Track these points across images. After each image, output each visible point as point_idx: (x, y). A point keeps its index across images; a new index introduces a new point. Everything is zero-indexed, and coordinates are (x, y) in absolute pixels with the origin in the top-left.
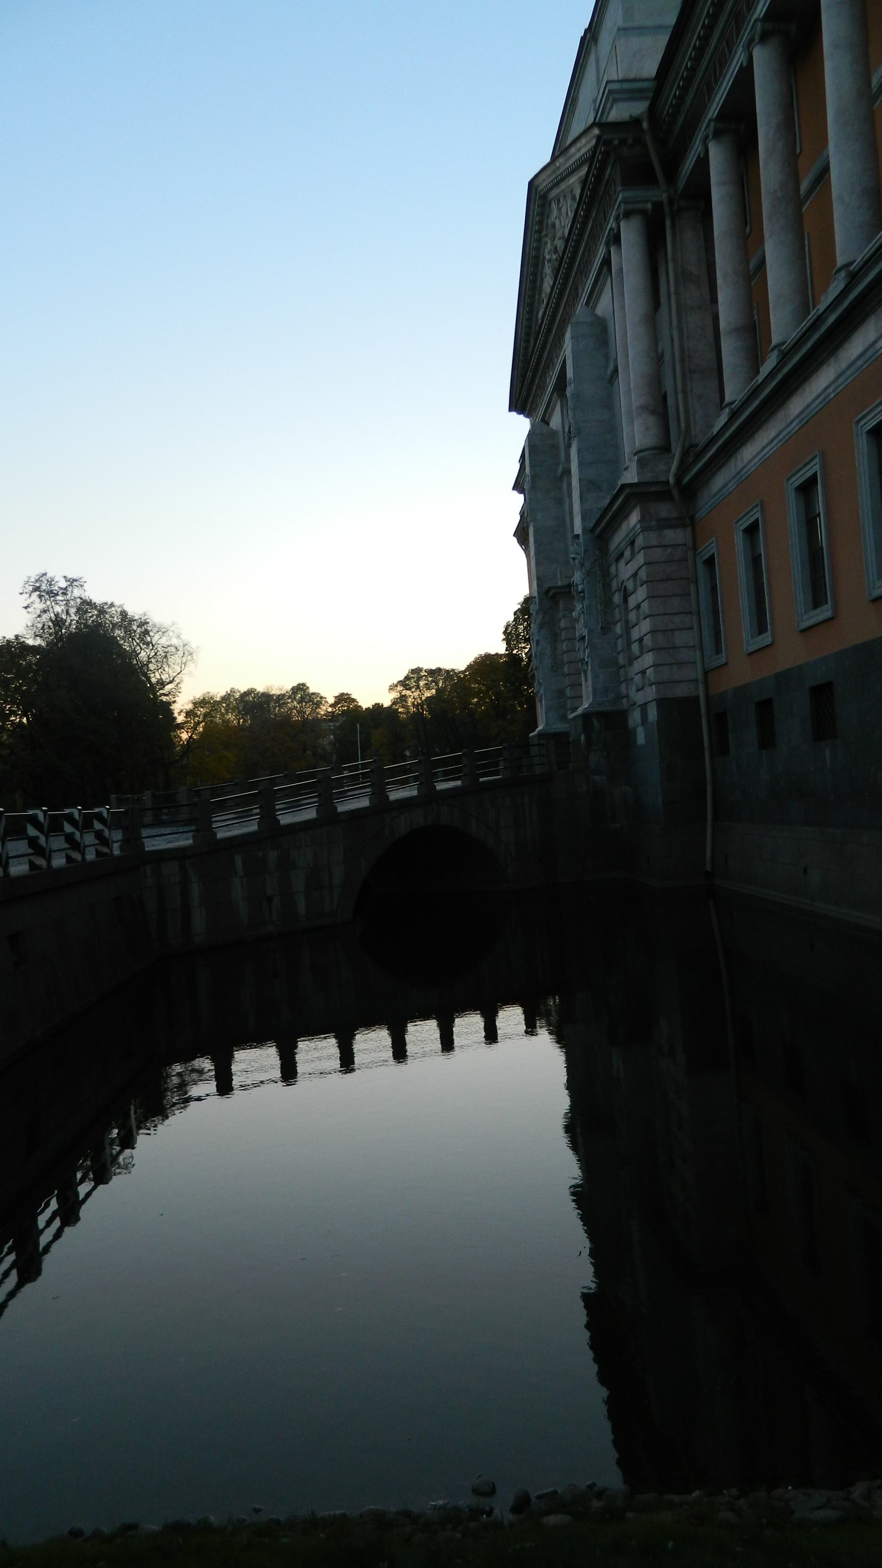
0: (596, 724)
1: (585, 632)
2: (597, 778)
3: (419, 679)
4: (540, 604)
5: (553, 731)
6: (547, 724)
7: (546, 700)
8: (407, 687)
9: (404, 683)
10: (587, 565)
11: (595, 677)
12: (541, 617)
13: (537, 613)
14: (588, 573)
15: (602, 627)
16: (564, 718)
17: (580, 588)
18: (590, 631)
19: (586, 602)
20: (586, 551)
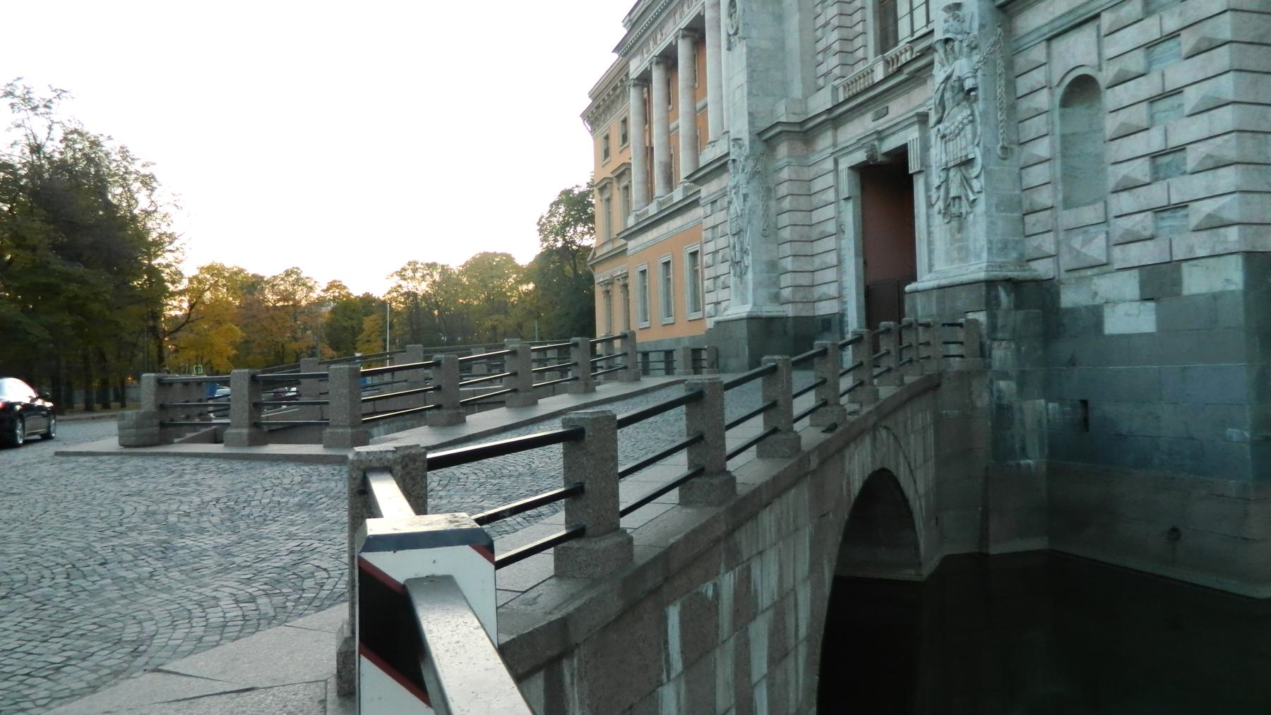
0: (1004, 297)
1: (977, 153)
2: (1002, 384)
3: (415, 271)
4: (751, 148)
5: (764, 314)
6: (755, 305)
7: (754, 273)
8: (404, 278)
9: (401, 274)
10: (985, 47)
11: (991, 224)
12: (751, 163)
13: (747, 158)
14: (985, 61)
15: (1003, 148)
16: (776, 298)
17: (968, 84)
18: (986, 152)
19: (979, 107)
20: (982, 26)
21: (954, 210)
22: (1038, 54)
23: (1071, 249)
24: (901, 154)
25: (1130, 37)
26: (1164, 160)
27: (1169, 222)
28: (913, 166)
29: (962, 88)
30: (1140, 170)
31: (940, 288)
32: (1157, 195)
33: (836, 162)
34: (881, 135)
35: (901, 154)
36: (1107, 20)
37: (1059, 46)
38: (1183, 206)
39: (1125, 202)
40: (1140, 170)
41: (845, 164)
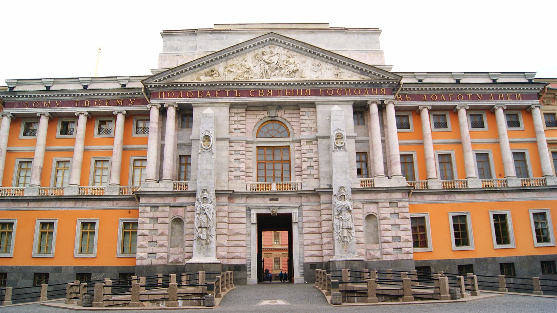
21: (345, 239)
22: (360, 205)
23: (370, 254)
24: (290, 215)
25: (386, 210)
26: (397, 238)
27: (398, 251)
28: (294, 219)
29: (349, 209)
30: (390, 239)
31: (346, 261)
32: (394, 245)
33: (249, 209)
34: (280, 208)
35: (290, 215)
36: (380, 205)
37: (366, 206)
38: (401, 248)
39: (386, 245)
40: (390, 239)
41: (254, 213)
